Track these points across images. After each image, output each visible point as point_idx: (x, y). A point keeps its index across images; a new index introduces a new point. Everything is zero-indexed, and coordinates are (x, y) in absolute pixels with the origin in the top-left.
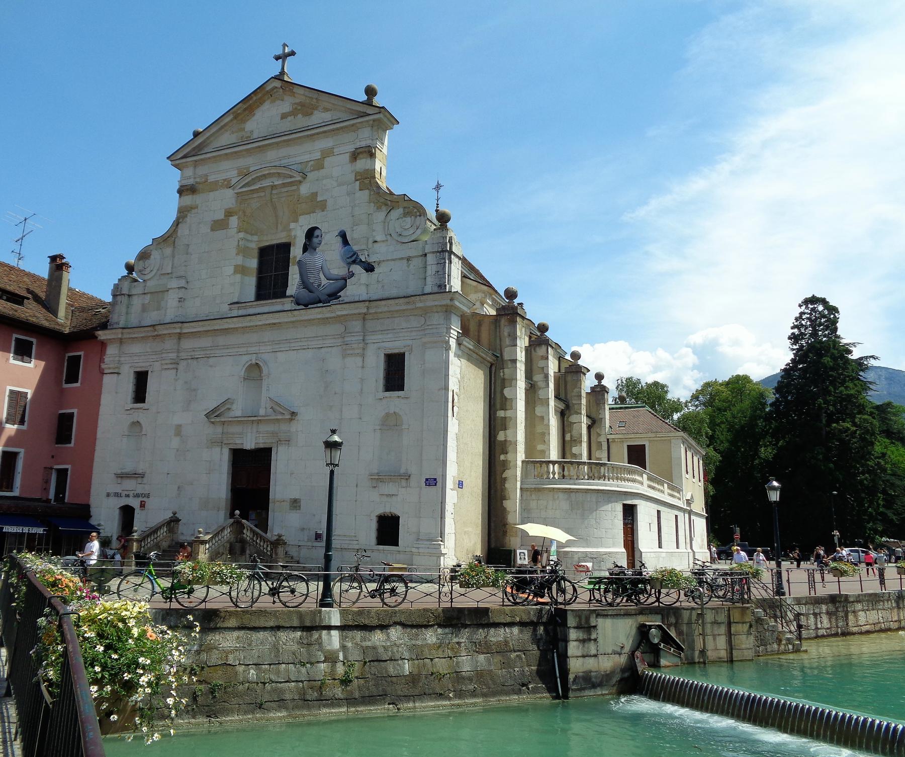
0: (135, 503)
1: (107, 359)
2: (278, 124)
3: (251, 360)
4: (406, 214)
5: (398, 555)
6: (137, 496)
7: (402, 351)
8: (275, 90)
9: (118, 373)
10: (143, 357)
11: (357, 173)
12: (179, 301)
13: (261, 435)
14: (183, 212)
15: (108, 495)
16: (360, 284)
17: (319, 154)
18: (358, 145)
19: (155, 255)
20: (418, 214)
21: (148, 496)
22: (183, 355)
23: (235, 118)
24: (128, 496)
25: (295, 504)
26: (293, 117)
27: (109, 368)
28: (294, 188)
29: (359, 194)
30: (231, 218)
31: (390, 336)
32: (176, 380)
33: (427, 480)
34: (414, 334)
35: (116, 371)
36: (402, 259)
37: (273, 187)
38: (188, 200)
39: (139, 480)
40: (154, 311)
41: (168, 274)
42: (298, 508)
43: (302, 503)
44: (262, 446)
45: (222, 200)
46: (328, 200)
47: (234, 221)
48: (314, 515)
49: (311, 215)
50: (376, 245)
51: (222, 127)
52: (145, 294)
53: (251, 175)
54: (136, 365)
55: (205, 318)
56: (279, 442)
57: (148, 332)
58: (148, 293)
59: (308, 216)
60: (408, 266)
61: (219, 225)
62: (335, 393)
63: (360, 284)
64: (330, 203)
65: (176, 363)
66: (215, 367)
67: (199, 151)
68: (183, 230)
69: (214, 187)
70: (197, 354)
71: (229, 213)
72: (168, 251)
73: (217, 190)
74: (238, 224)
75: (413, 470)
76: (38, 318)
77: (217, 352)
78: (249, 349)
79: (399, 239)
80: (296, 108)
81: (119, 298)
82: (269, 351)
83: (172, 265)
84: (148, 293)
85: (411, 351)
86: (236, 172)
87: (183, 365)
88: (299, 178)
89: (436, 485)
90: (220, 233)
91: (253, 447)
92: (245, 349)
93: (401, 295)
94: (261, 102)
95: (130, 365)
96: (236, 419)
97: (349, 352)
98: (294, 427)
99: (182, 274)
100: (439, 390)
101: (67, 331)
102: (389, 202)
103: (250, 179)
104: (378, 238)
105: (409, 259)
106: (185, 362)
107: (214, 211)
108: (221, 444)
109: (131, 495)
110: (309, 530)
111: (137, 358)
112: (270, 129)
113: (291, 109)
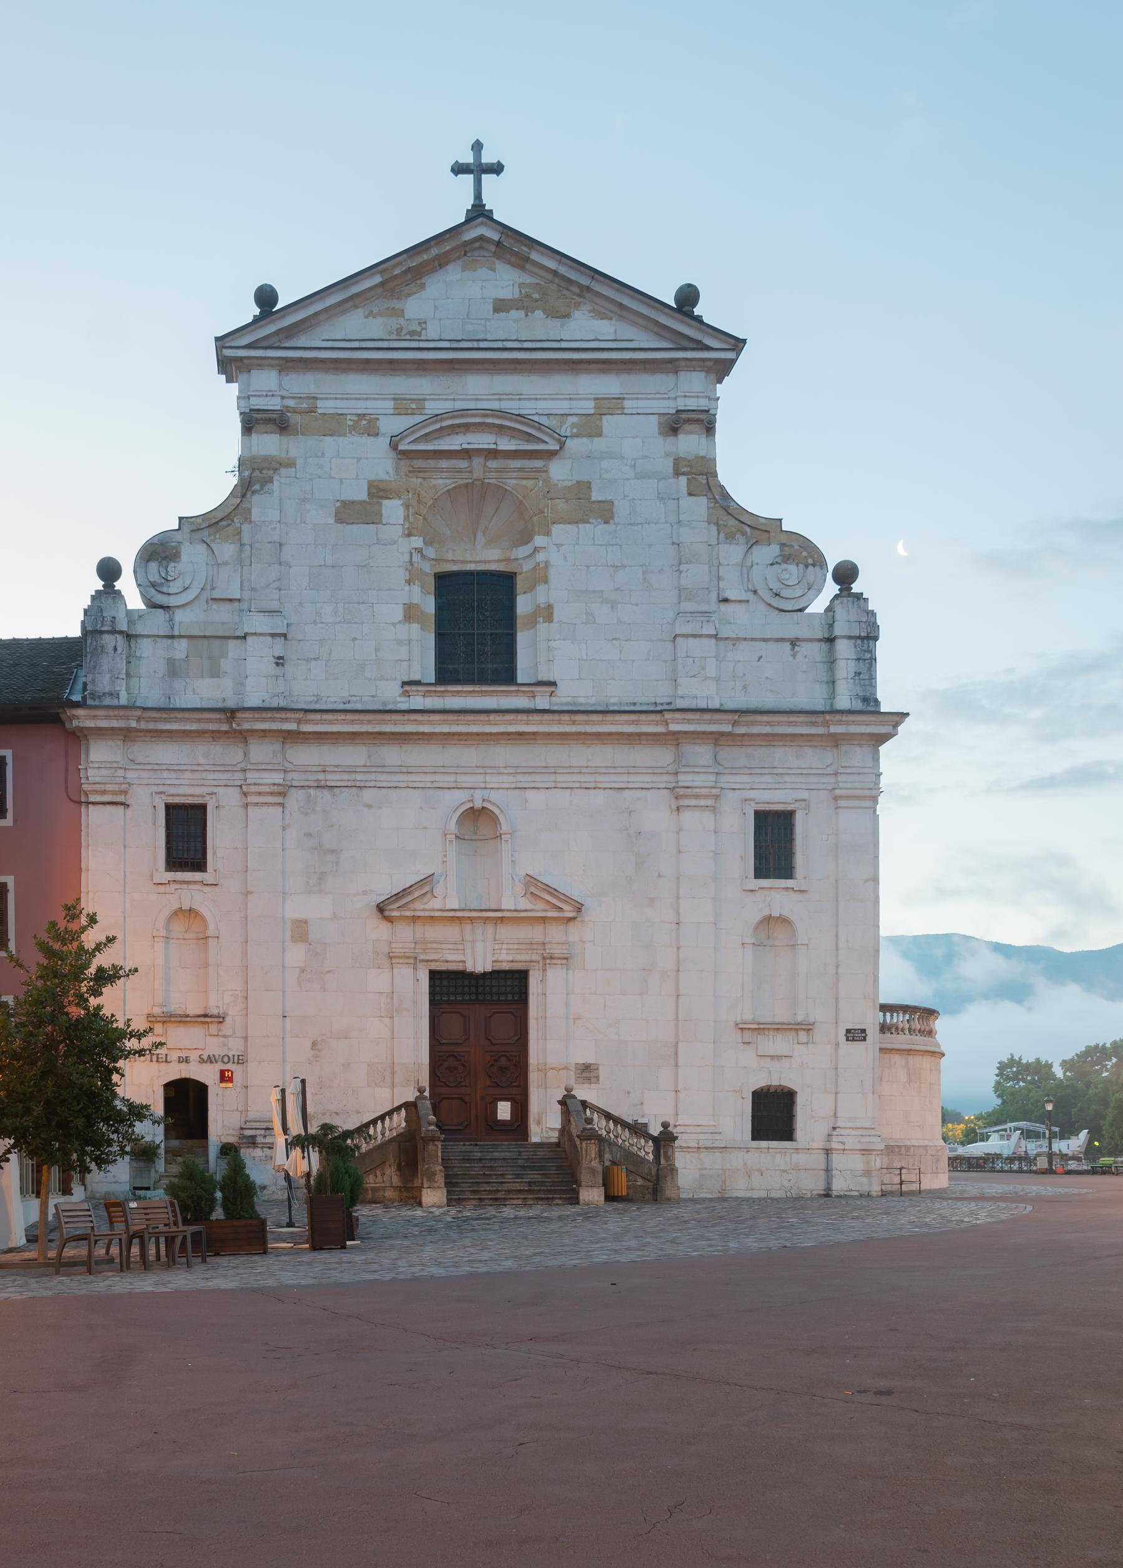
0: (207, 1075)
2: (488, 320)
4: (786, 558)
5: (794, 1155)
6: (211, 1060)
7: (790, 808)
8: (477, 244)
9: (126, 805)
10: (188, 775)
11: (677, 462)
12: (277, 664)
13: (505, 946)
14: (261, 470)
16: (706, 678)
17: (592, 404)
18: (682, 404)
19: (192, 555)
20: (810, 561)
21: (241, 1060)
22: (297, 778)
23: (382, 284)
24: (186, 1060)
25: (587, 1072)
26: (522, 313)
27: (103, 792)
28: (537, 464)
29: (687, 502)
30: (385, 502)
31: (768, 779)
32: (284, 829)
33: (848, 1031)
34: (813, 779)
36: (782, 640)
38: (269, 444)
39: (213, 1029)
40: (202, 677)
41: (231, 600)
42: (593, 1080)
43: (601, 1069)
44: (506, 966)
45: (359, 459)
46: (616, 502)
47: (393, 510)
48: (629, 1093)
49: (581, 526)
50: (724, 607)
51: (351, 298)
52: (172, 637)
53: (442, 420)
54: (172, 790)
55: (341, 707)
56: (548, 959)
57: (209, 721)
58: (180, 637)
59: (573, 527)
60: (794, 656)
62: (659, 876)
63: (706, 678)
64: (621, 510)
65: (281, 792)
66: (380, 808)
67: (289, 337)
68: (261, 507)
69: (334, 425)
70: (333, 779)
71: (379, 492)
72: (226, 550)
73: (344, 435)
74: (406, 518)
75: (820, 1014)
77: (384, 777)
78: (461, 778)
79: (776, 602)
80: (528, 296)
81: (108, 640)
82: (507, 786)
83: (242, 583)
84: (180, 637)
85: (807, 808)
86: (391, 404)
87: (295, 799)
89: (864, 1039)
90: (360, 531)
91: (489, 968)
92: (452, 778)
93: (784, 706)
94: (441, 262)
95: (155, 789)
96: (451, 914)
97: (686, 802)
98: (574, 933)
99: (275, 605)
100: (866, 881)
102: (748, 530)
103: (437, 426)
104: (730, 594)
105: (794, 642)
106: (302, 793)
107: (341, 480)
108: (414, 961)
109: (194, 1056)
111: (174, 775)
112: (469, 327)
113: (517, 295)
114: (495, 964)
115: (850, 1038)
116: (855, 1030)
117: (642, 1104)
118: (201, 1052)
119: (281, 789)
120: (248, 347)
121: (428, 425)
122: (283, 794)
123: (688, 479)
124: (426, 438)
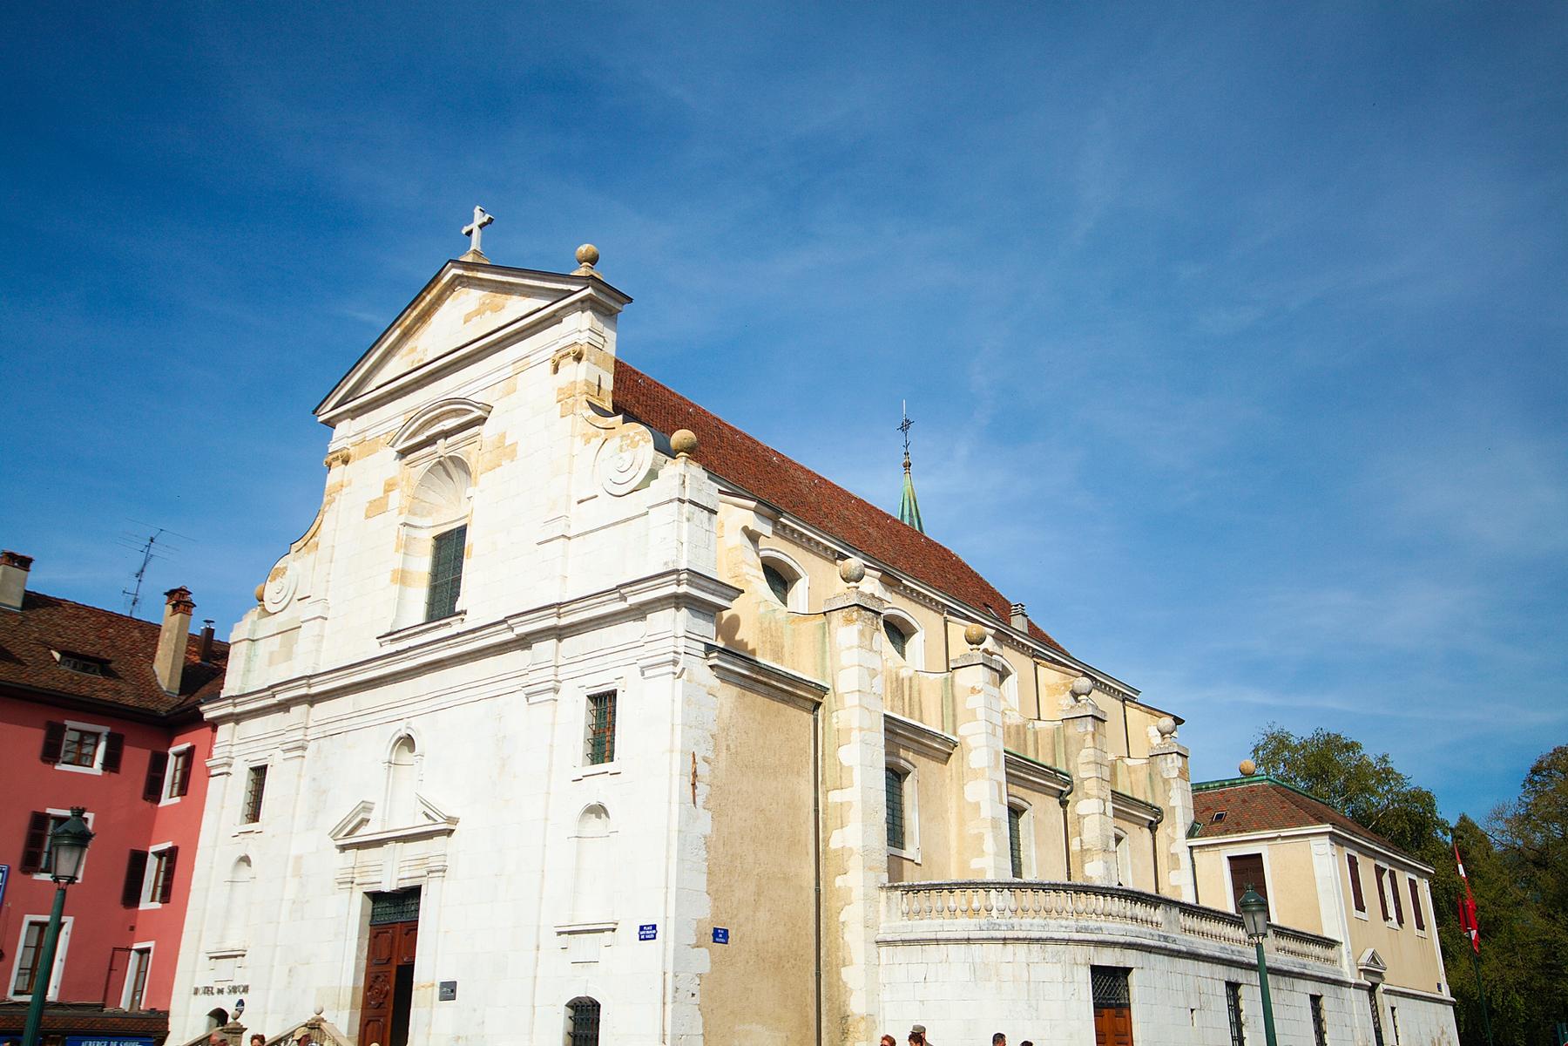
0: (228, 1004)
1: (216, 752)
3: (400, 730)
6: (234, 990)
15: (196, 992)
25: (449, 991)
35: (225, 769)
37: (446, 434)
47: (395, 498)
48: (475, 1010)
49: (497, 470)
61: (376, 508)
71: (390, 487)
76: (118, 692)
88: (478, 413)
89: (654, 938)
101: (163, 710)
109: (226, 990)
110: (466, 1038)
114: (400, 882)
115: (643, 937)
116: (647, 926)
117: (483, 1022)
118: (229, 983)
119: (300, 744)
120: (332, 410)
121: (410, 426)
122: (304, 748)
123: (562, 405)
124: (413, 435)
